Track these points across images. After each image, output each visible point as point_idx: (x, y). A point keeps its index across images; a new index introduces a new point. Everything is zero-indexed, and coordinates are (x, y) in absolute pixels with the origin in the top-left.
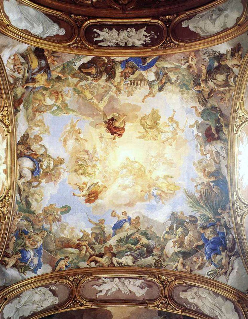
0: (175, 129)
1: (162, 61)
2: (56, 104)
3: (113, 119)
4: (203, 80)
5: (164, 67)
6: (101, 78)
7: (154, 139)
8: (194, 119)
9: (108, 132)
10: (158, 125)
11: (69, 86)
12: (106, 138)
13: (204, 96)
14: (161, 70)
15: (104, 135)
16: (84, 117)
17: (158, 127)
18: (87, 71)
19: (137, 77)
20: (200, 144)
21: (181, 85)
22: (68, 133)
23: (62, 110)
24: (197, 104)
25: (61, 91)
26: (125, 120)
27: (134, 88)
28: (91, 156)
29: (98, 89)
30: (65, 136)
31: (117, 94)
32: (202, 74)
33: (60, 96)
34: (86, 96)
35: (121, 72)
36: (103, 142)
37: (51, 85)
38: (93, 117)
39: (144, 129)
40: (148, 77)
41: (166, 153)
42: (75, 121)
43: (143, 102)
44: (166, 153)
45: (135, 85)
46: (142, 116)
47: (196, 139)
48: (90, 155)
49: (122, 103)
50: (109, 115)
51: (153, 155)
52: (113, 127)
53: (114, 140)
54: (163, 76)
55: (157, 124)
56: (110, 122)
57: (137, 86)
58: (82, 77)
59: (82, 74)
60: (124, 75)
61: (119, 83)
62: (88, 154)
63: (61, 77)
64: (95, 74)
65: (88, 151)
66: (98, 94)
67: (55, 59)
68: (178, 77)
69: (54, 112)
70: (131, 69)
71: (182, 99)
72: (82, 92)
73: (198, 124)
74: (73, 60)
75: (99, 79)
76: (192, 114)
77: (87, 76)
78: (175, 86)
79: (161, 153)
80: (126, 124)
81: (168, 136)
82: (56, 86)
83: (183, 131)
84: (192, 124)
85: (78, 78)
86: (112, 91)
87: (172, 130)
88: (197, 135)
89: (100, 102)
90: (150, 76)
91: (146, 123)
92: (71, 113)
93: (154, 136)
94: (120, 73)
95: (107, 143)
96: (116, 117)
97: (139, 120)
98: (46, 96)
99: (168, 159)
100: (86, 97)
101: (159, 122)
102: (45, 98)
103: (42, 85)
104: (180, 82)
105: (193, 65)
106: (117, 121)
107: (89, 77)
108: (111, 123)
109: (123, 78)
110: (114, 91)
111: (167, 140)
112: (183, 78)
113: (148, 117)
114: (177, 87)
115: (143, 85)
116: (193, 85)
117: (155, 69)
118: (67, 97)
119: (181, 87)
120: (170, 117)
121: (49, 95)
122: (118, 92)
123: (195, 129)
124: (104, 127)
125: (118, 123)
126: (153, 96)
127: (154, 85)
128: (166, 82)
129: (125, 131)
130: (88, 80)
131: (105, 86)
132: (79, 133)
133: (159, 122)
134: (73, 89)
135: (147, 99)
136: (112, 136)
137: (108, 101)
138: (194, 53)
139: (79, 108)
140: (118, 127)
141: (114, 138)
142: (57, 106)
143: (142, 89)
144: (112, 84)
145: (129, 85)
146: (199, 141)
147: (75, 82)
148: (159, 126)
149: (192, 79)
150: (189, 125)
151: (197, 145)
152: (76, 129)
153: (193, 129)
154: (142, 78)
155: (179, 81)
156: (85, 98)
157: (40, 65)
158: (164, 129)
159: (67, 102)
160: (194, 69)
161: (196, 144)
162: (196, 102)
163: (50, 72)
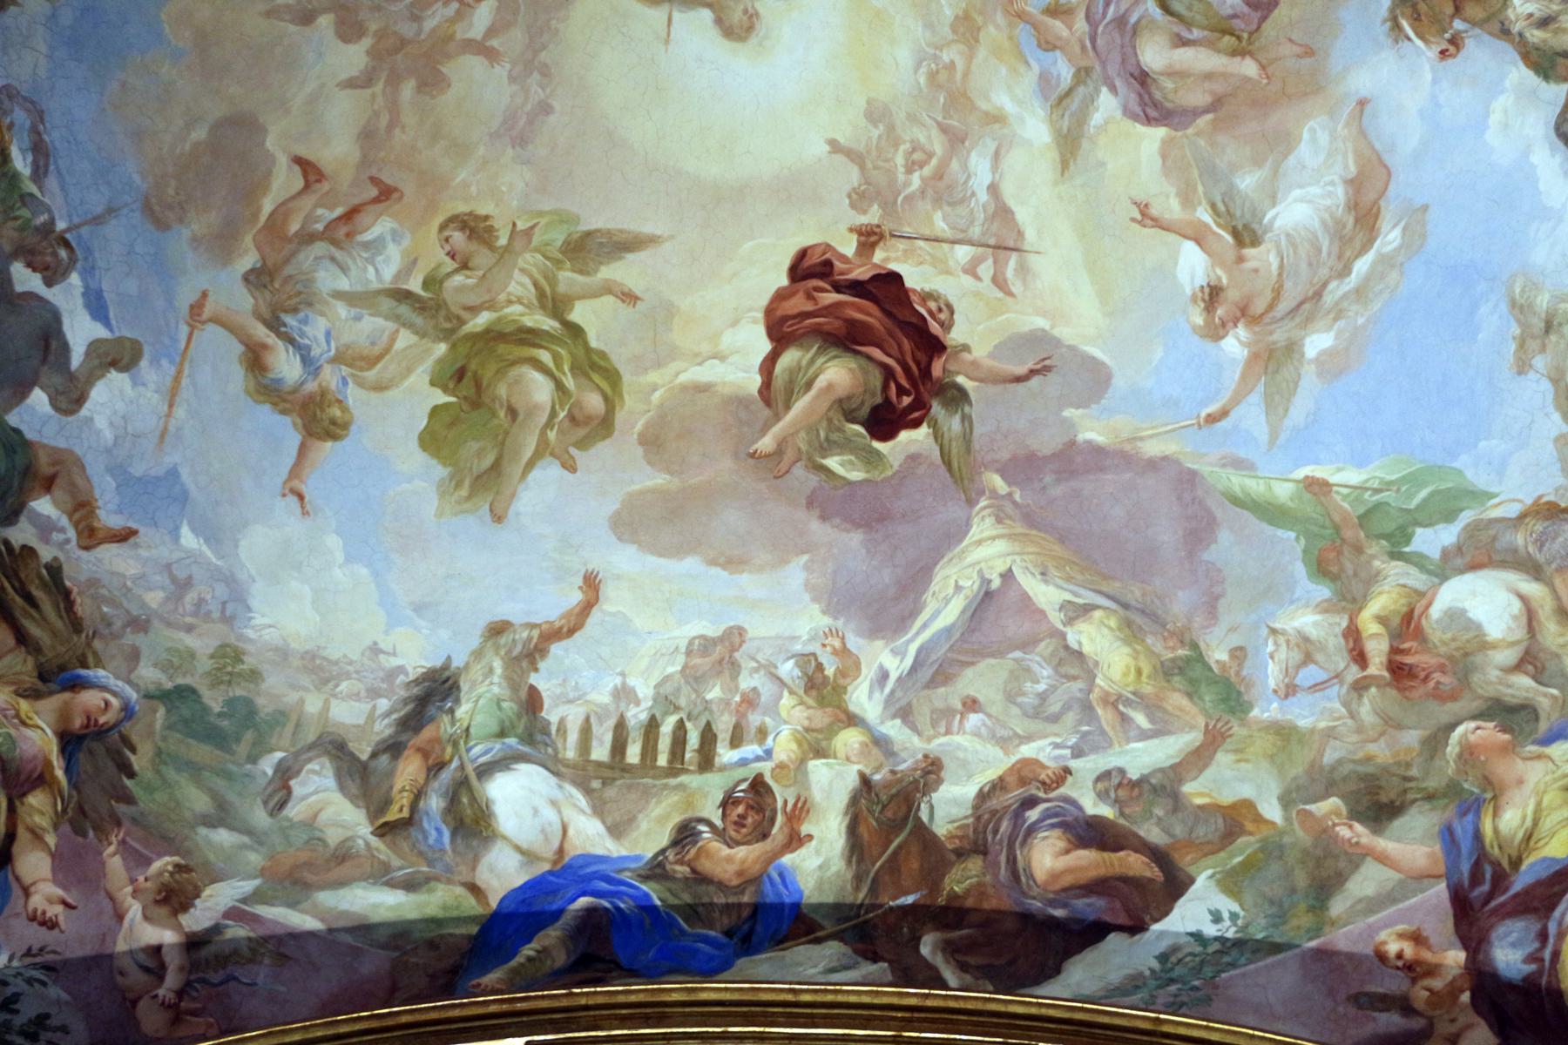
0: (274, 325)
1: (432, 944)
2: (1416, 579)
3: (884, 422)
4: (41, 779)
5: (410, 885)
6: (982, 797)
7: (474, 227)
8: (101, 423)
9: (932, 305)
10: (440, 361)
11: (1284, 733)
12: (954, 242)
13: (22, 638)
14: (430, 863)
15: (971, 270)
16: (1153, 449)
17: (442, 348)
18: (1106, 855)
19: (647, 793)
20: (15, 177)
21: (249, 736)
22: (1329, 299)
23: (1361, 517)
24: (82, 566)
25: (1360, 687)
26: (767, 412)
27: (682, 702)
28: (1104, 64)
29: (1011, 697)
30: (1362, 266)
31: (835, 652)
32: (51, 840)
33: (1378, 649)
34: (1126, 642)
35: (795, 840)
36: (983, 196)
37: (1452, 749)
38: (1072, 443)
39: (576, 331)
40: (554, 803)
41: (351, 84)
42: (1251, 415)
43: (592, 585)
44: (351, 84)
45: (667, 727)
46: (603, 449)
47: (61, 225)
48: (1113, 70)
49: (795, 574)
50: (913, 459)
51: (474, 64)
52: (876, 353)
53: (872, 216)
54: (414, 807)
55: (456, 376)
56: (906, 400)
57: (652, 726)
58: (1159, 812)
59: (1153, 834)
60: (772, 821)
61: (816, 746)
62: (1142, 78)
63: (1356, 815)
64: (1032, 830)
65: (1134, 117)
66: (1018, 654)
67: (1393, 984)
68: (282, 805)
69: (1443, 508)
70: (706, 866)
71: (235, 600)
72: (1169, 671)
73: (57, 380)
74: (1233, 965)
75: (999, 785)
76: (119, 471)
77: (1107, 811)
78: (298, 725)
79: (408, 89)
80: (757, 381)
81: (338, 254)
82: (1412, 738)
83: (196, 309)
84: (114, 375)
85: (1199, 801)
86: (884, 676)
87: (305, 321)
88: (52, 275)
89: (996, 583)
90: (536, 811)
91: (559, 386)
92: (1283, 492)
93: (483, 258)
94: (810, 837)
95: (943, 190)
96: (845, 446)
97: (634, 414)
98: (1507, 656)
99: (325, 21)
100: (1131, 632)
101: (442, 398)
102: (1520, 634)
103: (1539, 757)
104: (253, 759)
105: (146, 918)
106: (840, 401)
107: (1093, 806)
108: (902, 391)
109: (782, 795)
110: (868, 673)
111: (350, 215)
112: (231, 797)
113: (543, 433)
114: (280, 717)
115: (596, 729)
116: (135, 732)
117: (492, 870)
118: (1306, 639)
119: (245, 714)
120: (329, 444)
121: (1478, 659)
122: (830, 671)
123: (81, 332)
124: (966, 348)
125: (830, 387)
126: (497, 630)
127: (495, 728)
128: (384, 759)
129: (769, 312)
130: (1098, 779)
131: (945, 718)
132: (1213, 295)
133: (442, 398)
134: (1251, 706)
135: (558, 601)
136: (886, 258)
137: (925, 590)
138: (136, 1024)
139: (1199, 530)
140: (834, 352)
141: (870, 238)
142: (1418, 560)
143: (603, 697)
144: (880, 742)
145: (723, 726)
146: (25, 213)
147: (1223, 758)
148: (429, 363)
149: (150, 789)
150: (144, 363)
151: (39, 174)
152: (1242, 331)
153: (101, 332)
154: (611, 792)
155: (268, 765)
156: (1139, 619)
157: (1543, 936)
158: (390, 326)
159: (1311, 586)
160: (133, 881)
161: (52, 182)
162: (93, 583)
163: (1450, 875)
